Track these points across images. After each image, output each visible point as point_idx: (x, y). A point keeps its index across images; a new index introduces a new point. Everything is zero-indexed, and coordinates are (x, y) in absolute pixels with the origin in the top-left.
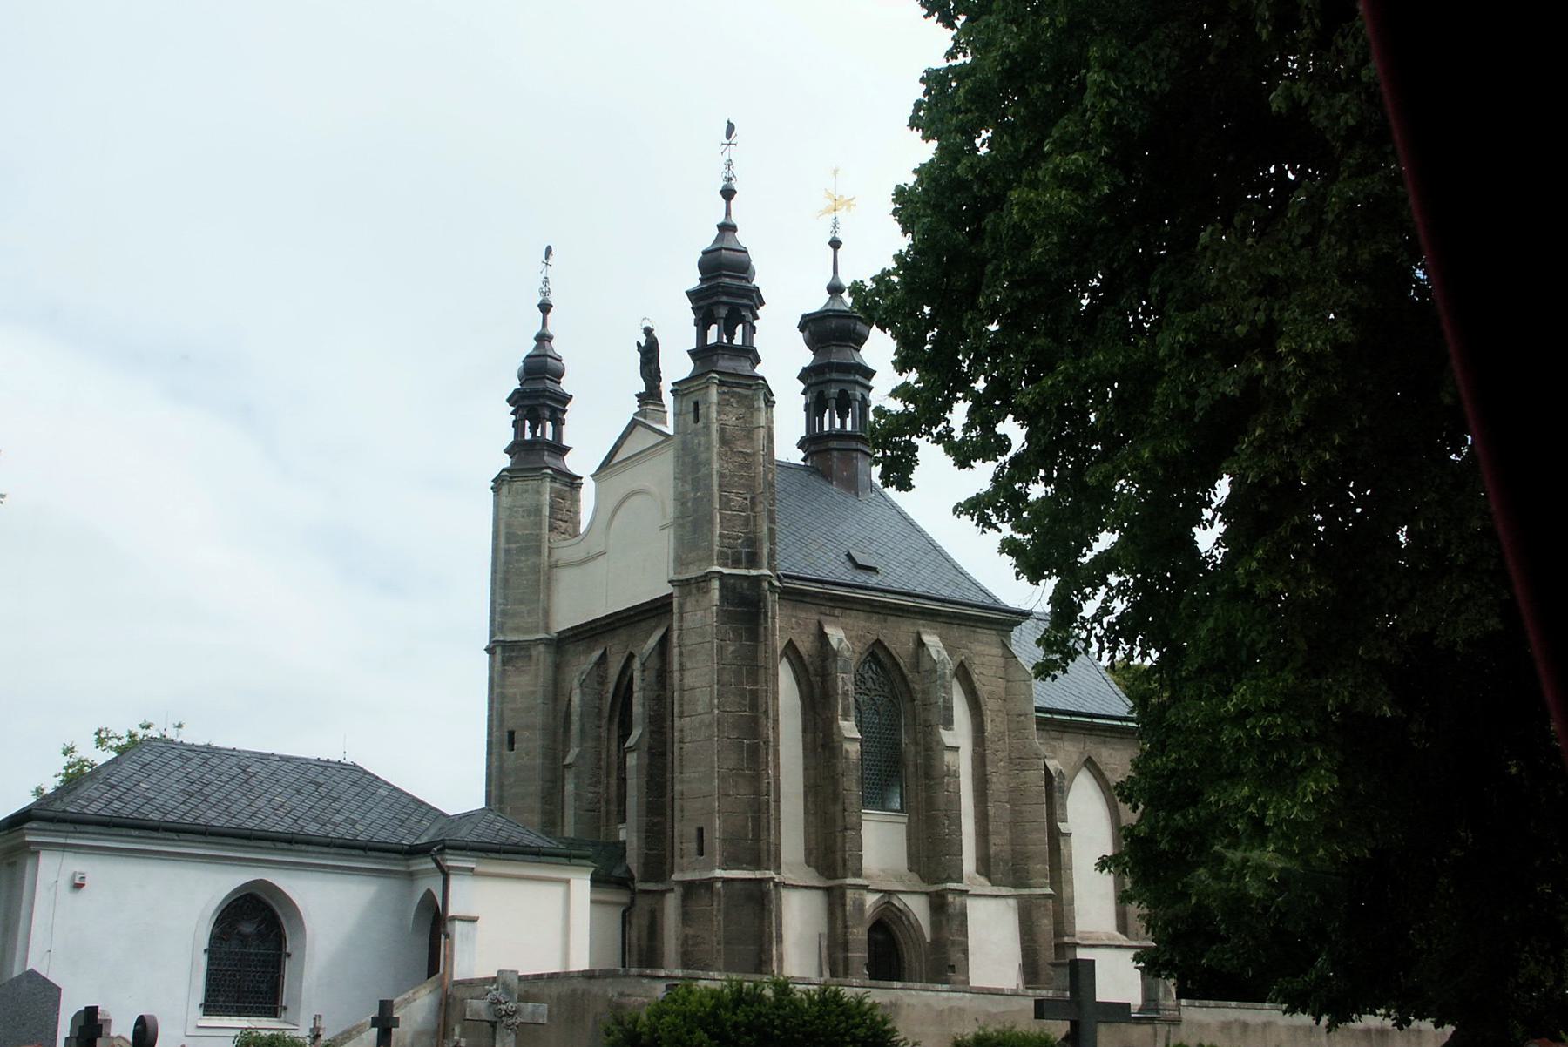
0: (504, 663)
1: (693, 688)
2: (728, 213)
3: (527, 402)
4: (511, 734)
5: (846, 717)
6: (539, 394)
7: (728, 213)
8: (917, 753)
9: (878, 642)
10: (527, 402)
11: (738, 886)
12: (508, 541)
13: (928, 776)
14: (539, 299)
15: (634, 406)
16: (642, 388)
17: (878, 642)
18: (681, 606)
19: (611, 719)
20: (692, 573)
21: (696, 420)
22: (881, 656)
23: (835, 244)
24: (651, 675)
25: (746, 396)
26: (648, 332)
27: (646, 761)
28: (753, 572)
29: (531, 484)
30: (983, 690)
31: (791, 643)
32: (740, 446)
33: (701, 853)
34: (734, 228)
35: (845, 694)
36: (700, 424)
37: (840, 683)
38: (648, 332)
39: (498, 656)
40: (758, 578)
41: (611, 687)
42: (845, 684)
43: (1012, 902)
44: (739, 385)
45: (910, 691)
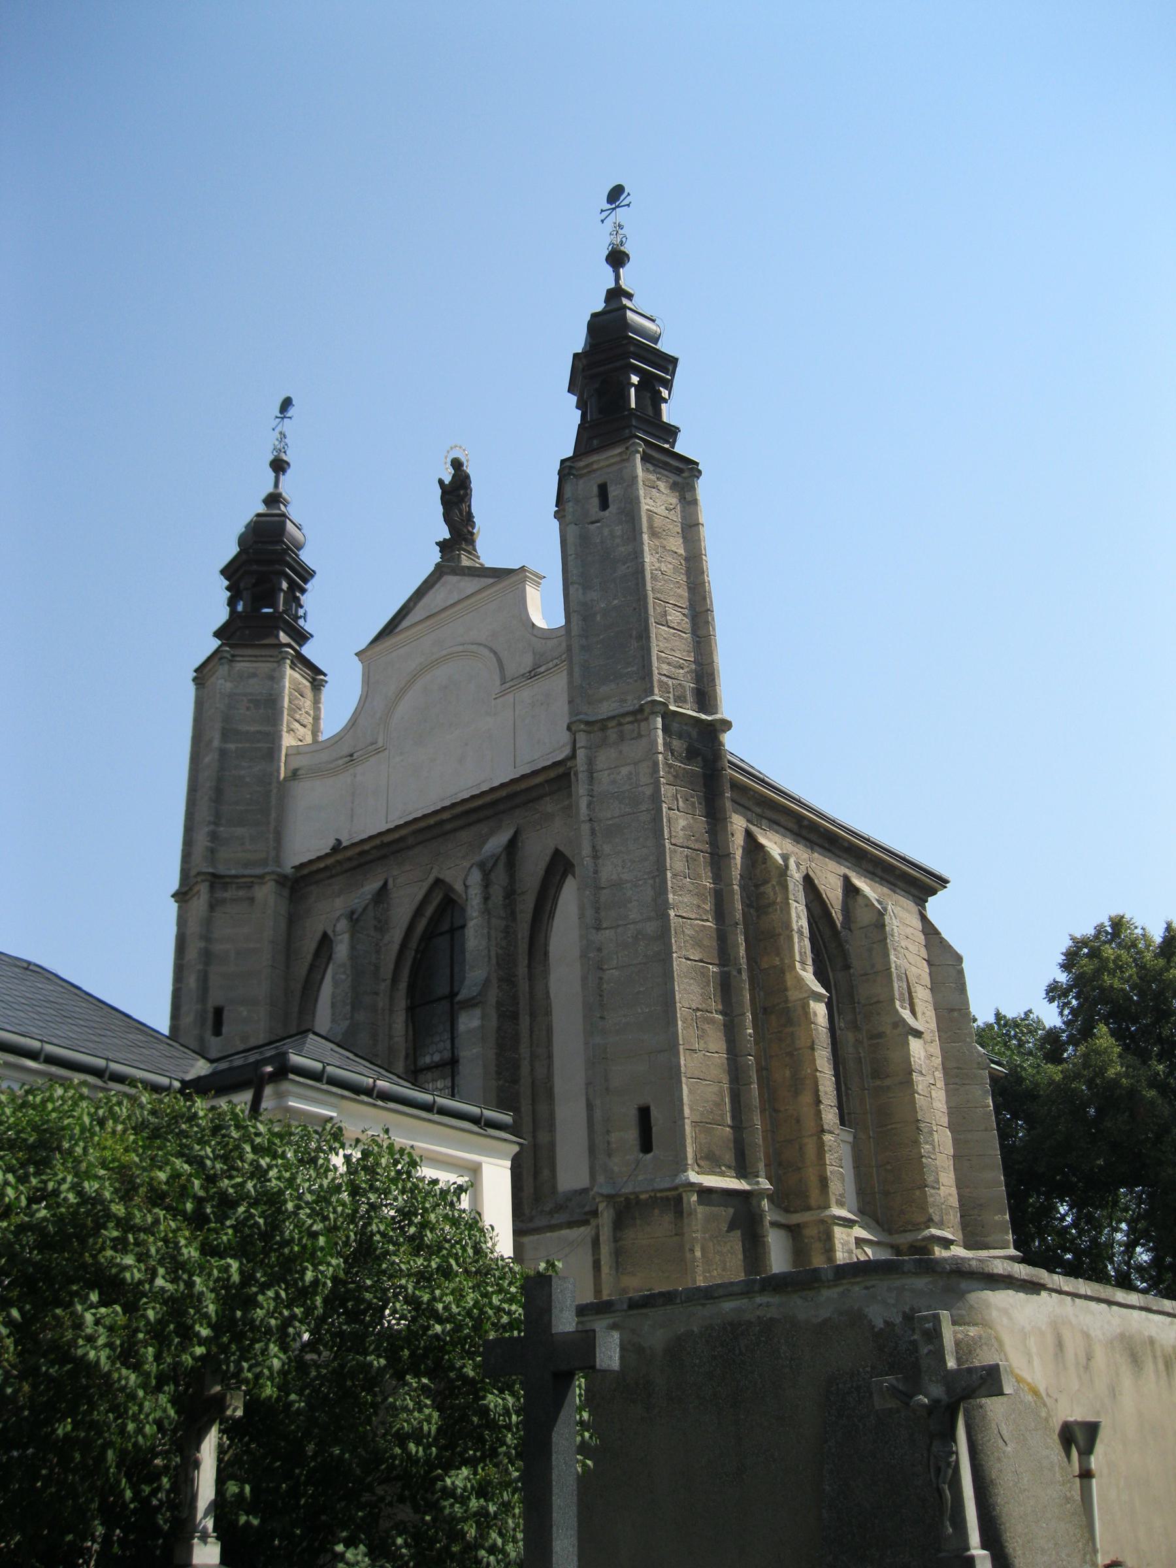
0: (212, 907)
1: (618, 885)
2: (617, 278)
3: (255, 567)
4: (219, 1012)
6: (266, 575)
8: (858, 1042)
10: (255, 567)
12: (226, 735)
13: (876, 1074)
14: (271, 457)
15: (435, 556)
16: (444, 533)
18: (590, 762)
19: (395, 980)
20: (606, 709)
21: (604, 505)
24: (497, 892)
26: (457, 464)
27: (493, 1022)
28: (704, 717)
29: (264, 667)
33: (646, 1145)
35: (801, 933)
36: (613, 508)
38: (457, 464)
39: (200, 904)
41: (396, 936)
45: (844, 955)
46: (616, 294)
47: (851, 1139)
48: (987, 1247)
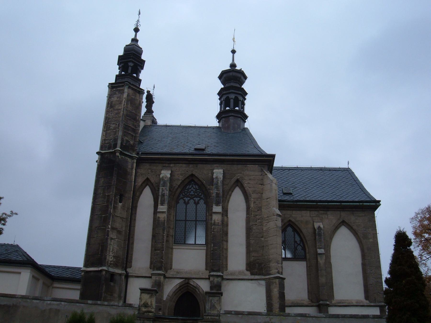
2: (136, 36)
5: (162, 204)
7: (136, 36)
9: (192, 175)
11: (92, 273)
17: (192, 175)
22: (196, 180)
23: (233, 52)
25: (122, 90)
30: (249, 190)
31: (148, 179)
32: (117, 107)
34: (137, 41)
35: (163, 195)
37: (161, 190)
40: (114, 153)
42: (163, 191)
43: (263, 283)
44: (119, 87)
46: (135, 40)
47: (205, 248)
48: (270, 274)
